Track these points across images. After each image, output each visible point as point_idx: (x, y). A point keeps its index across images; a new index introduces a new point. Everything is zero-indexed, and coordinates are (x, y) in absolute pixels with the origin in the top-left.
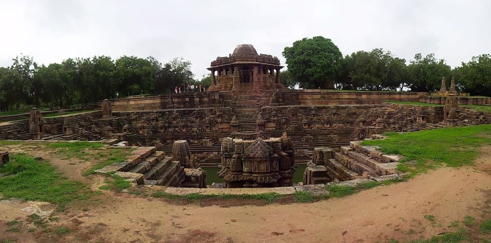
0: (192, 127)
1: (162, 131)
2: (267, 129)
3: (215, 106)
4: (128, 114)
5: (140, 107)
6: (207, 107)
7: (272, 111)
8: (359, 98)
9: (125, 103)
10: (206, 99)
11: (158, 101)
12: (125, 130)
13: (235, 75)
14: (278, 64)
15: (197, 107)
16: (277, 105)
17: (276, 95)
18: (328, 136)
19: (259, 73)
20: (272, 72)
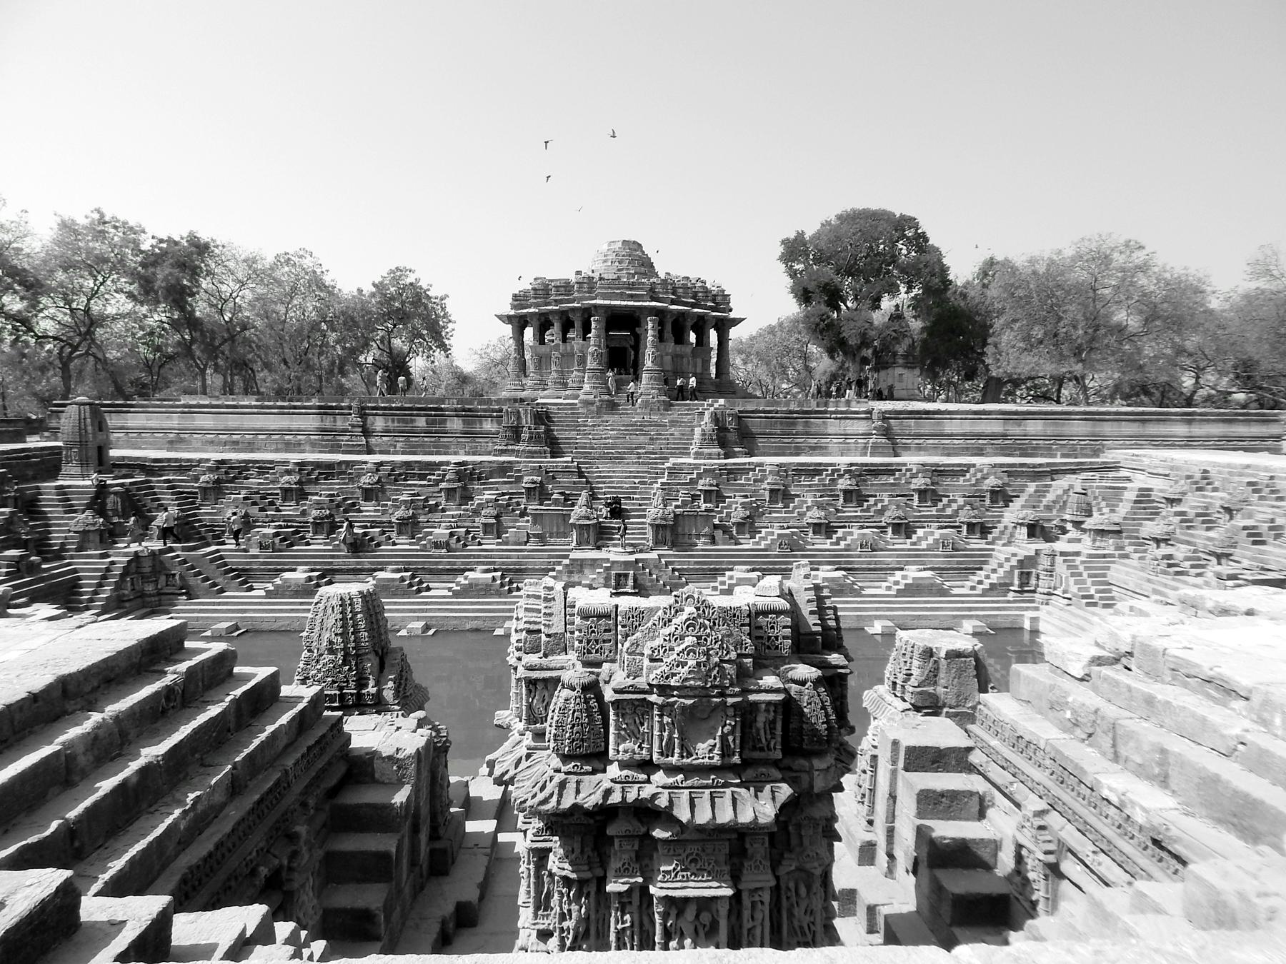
5: (236, 443)
7: (700, 476)
8: (1014, 429)
9: (175, 421)
10: (488, 426)
11: (310, 422)
15: (456, 453)
17: (716, 419)
18: (898, 573)
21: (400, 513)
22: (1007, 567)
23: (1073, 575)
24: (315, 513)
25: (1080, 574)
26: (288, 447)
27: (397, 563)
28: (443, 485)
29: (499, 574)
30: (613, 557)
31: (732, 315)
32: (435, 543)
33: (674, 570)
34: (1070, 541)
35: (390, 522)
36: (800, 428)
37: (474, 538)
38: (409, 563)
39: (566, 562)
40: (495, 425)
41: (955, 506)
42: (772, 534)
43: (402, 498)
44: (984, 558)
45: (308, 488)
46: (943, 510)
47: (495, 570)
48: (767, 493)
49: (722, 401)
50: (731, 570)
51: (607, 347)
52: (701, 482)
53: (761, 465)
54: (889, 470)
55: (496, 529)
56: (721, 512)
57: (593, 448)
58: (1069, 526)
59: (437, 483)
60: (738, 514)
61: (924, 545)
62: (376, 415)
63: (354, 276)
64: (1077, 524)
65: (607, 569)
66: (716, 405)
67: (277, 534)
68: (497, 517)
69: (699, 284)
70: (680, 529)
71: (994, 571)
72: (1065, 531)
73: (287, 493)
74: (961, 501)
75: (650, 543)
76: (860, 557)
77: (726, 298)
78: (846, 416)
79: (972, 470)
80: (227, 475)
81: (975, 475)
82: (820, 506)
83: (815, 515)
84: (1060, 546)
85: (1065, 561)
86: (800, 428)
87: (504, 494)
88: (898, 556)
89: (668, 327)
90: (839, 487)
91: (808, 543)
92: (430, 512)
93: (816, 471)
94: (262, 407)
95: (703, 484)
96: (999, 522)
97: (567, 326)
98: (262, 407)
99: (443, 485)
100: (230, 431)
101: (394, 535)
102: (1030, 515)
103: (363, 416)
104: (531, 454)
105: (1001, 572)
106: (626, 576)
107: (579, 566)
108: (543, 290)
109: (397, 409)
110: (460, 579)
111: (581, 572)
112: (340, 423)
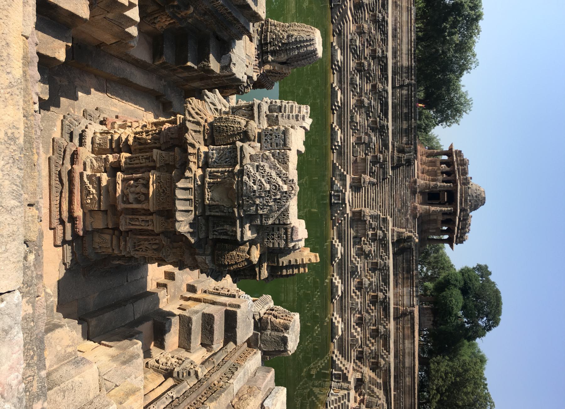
3: (393, 152)
7: (383, 231)
10: (405, 139)
14: (456, 241)
15: (393, 125)
16: (393, 239)
17: (410, 237)
20: (444, 232)
22: (343, 368)
23: (339, 398)
24: (366, 63)
25: (340, 402)
27: (344, 99)
28: (378, 119)
29: (340, 144)
30: (347, 194)
31: (454, 245)
32: (353, 116)
33: (342, 220)
34: (355, 398)
35: (362, 96)
36: (405, 276)
37: (355, 133)
38: (344, 105)
39: (345, 173)
40: (405, 142)
41: (370, 345)
42: (358, 263)
43: (372, 101)
44: (348, 359)
45: (376, 60)
46: (369, 340)
47: (341, 143)
48: (376, 261)
49: (417, 240)
50: (342, 246)
51: (440, 191)
52: (381, 232)
53: (389, 258)
54: (387, 315)
55: (359, 142)
56: (367, 241)
57: (396, 184)
58: (362, 397)
59: (379, 117)
60: (367, 248)
61: (353, 331)
62: (408, 91)
63: (469, 83)
64: (362, 401)
65: (342, 191)
66: (415, 238)
68: (364, 142)
69: (467, 230)
70: (360, 223)
71: (341, 362)
72: (360, 395)
73: (374, 51)
74: (373, 348)
75: (353, 210)
76: (348, 302)
77: (461, 242)
79: (387, 353)
80: (381, 25)
81: (385, 354)
82: (371, 284)
83: (366, 282)
84: (353, 393)
85: (345, 394)
87: (374, 145)
88: (348, 320)
90: (379, 293)
91: (354, 280)
92: (367, 114)
93: (387, 283)
94: (411, 42)
95: (380, 233)
96: (364, 365)
97: (448, 173)
98: (411, 42)
99: (378, 119)
101: (356, 98)
102: (367, 380)
103: (408, 85)
104: (392, 158)
105: (341, 365)
106: (339, 200)
109: (411, 100)
110: (337, 127)
111: (341, 180)
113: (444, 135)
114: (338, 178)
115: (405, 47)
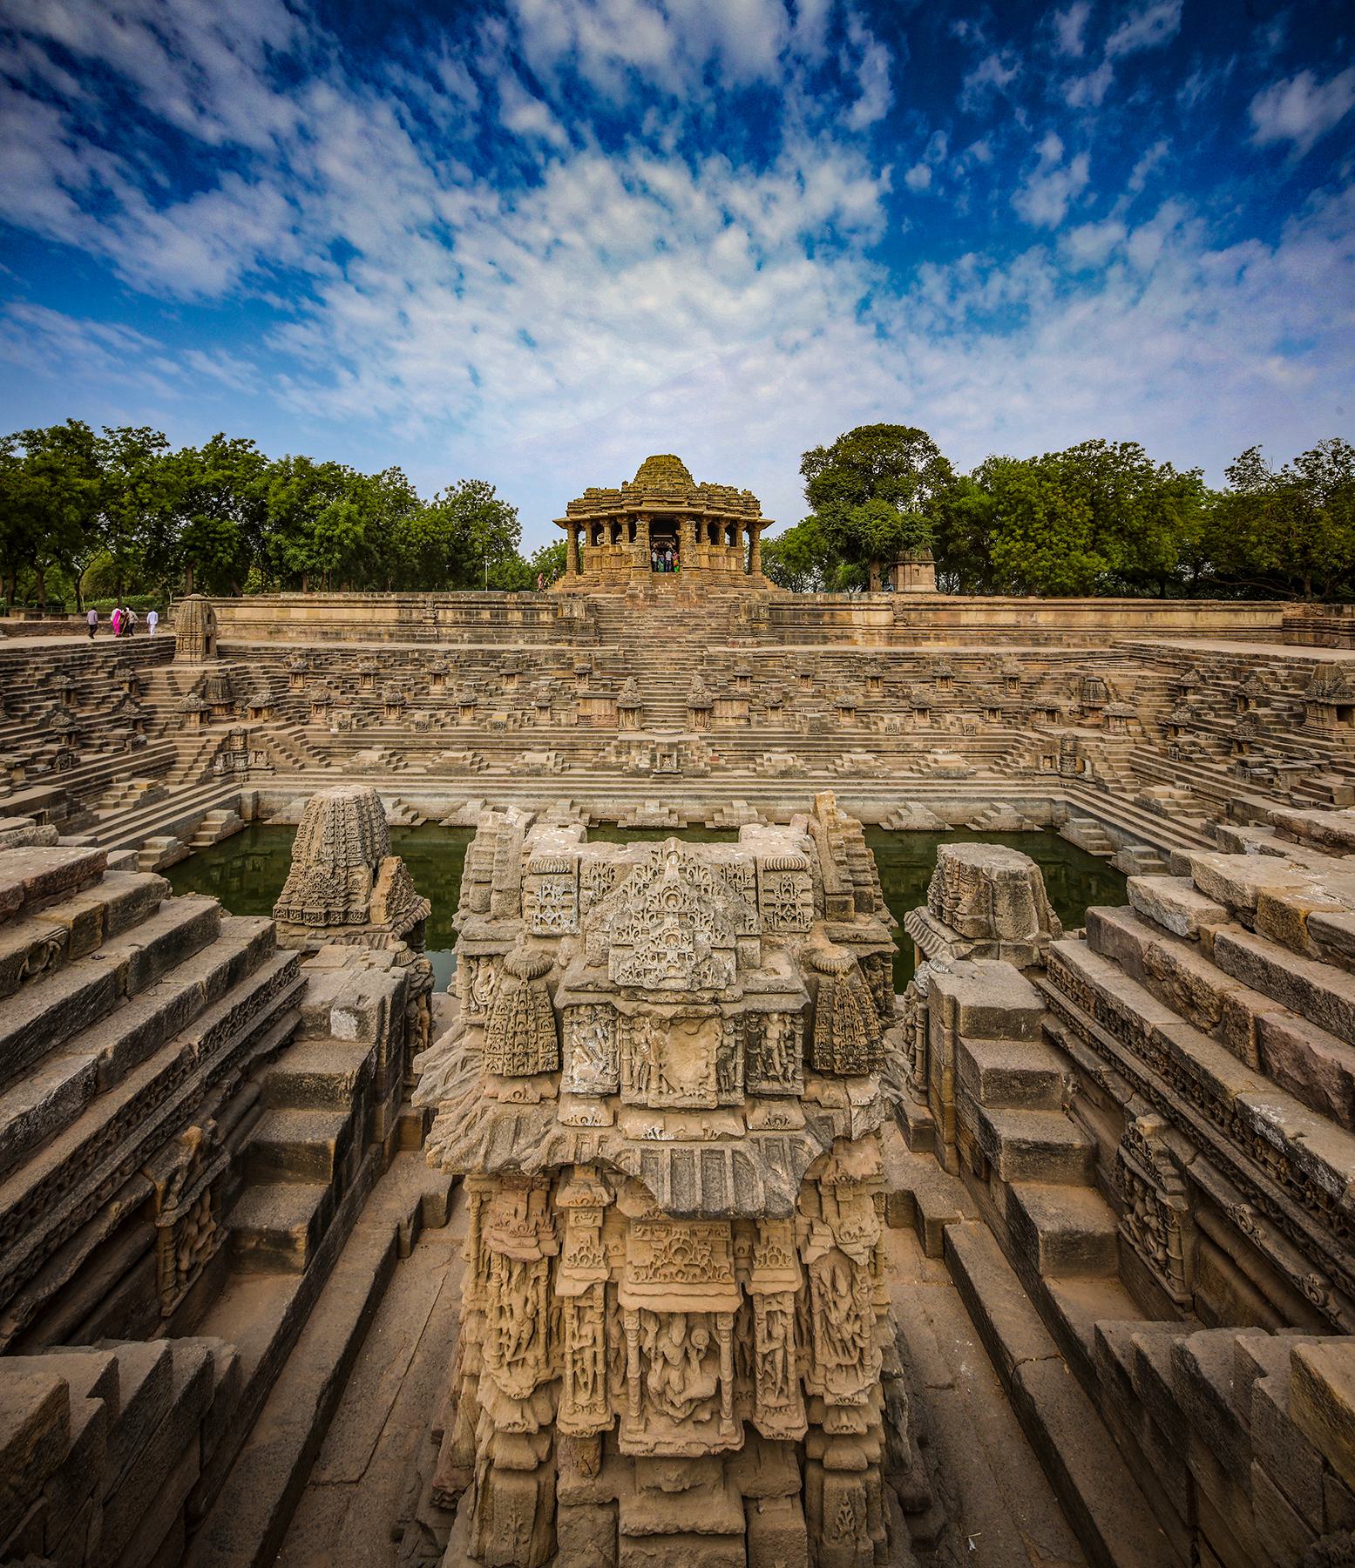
0: (492, 707)
1: (393, 716)
2: (719, 722)
3: (570, 642)
4: (278, 655)
6: (546, 642)
9: (275, 614)
12: (258, 711)
13: (637, 548)
19: (698, 540)
21: (464, 697)
26: (370, 637)
28: (503, 671)
30: (658, 739)
67: (353, 716)
78: (869, 607)
86: (826, 619)
89: (705, 530)
97: (616, 530)
99: (503, 671)
100: (320, 623)
104: (582, 644)
107: (624, 748)
108: (594, 497)
112: (415, 615)
113: (537, 536)
114: (623, 759)
115: (360, 614)
